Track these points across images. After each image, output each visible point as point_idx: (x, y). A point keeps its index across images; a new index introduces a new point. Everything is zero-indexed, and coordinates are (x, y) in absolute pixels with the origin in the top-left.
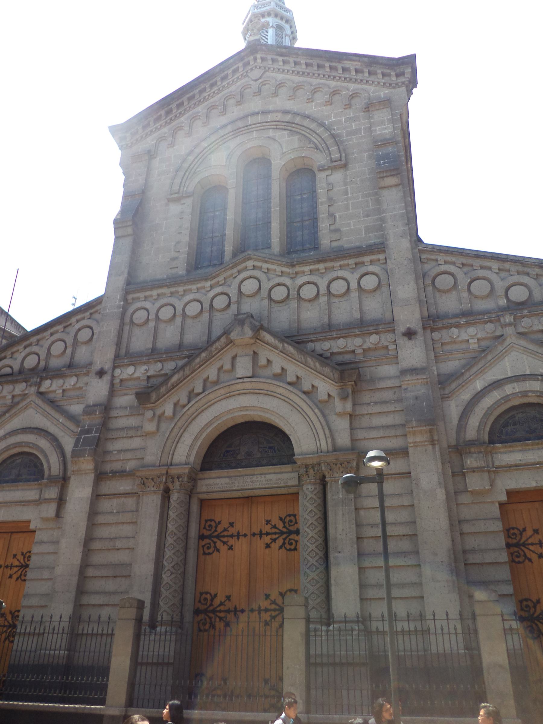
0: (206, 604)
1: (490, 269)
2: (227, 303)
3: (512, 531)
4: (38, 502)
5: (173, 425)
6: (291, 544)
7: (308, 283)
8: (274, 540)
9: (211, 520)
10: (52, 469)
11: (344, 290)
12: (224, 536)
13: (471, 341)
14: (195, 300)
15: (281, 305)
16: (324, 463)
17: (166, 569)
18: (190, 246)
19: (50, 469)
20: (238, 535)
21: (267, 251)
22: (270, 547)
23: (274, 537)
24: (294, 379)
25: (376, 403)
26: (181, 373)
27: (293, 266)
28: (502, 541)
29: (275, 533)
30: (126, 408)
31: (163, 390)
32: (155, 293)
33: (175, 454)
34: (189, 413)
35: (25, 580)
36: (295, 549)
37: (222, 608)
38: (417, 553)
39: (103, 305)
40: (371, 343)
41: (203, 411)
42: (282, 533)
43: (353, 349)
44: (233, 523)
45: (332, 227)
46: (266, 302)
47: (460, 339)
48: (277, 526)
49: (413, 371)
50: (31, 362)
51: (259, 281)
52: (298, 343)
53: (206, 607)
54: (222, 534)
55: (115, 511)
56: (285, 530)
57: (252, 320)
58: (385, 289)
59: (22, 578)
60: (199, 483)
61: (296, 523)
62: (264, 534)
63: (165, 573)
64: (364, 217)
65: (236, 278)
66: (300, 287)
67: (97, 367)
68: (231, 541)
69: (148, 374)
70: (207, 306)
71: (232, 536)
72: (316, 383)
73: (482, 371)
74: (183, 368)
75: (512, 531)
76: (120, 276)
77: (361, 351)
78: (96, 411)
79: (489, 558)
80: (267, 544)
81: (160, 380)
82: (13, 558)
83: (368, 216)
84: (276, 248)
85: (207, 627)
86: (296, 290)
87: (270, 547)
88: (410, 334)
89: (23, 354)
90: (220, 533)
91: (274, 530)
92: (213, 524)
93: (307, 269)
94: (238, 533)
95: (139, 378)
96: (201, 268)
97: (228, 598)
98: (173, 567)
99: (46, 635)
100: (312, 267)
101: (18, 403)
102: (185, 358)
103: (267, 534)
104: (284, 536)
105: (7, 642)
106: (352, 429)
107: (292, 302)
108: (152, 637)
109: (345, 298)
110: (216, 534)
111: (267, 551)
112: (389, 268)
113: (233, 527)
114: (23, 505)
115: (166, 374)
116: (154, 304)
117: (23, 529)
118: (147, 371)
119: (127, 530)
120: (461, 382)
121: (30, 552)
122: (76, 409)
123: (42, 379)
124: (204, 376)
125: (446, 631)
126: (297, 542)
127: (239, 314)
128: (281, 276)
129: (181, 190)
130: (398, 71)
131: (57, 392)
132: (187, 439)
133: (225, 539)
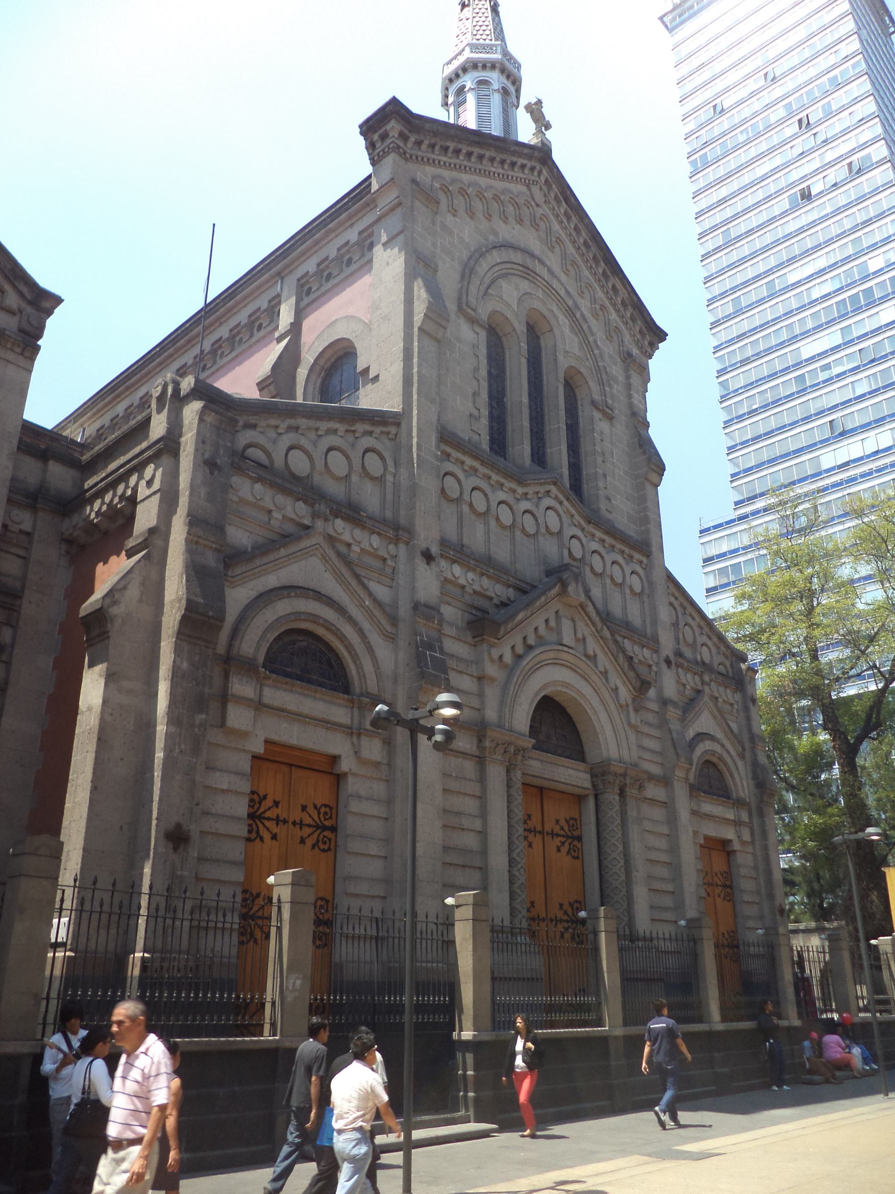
27: (589, 522)
50: (299, 463)
99: (391, 940)
114: (328, 728)
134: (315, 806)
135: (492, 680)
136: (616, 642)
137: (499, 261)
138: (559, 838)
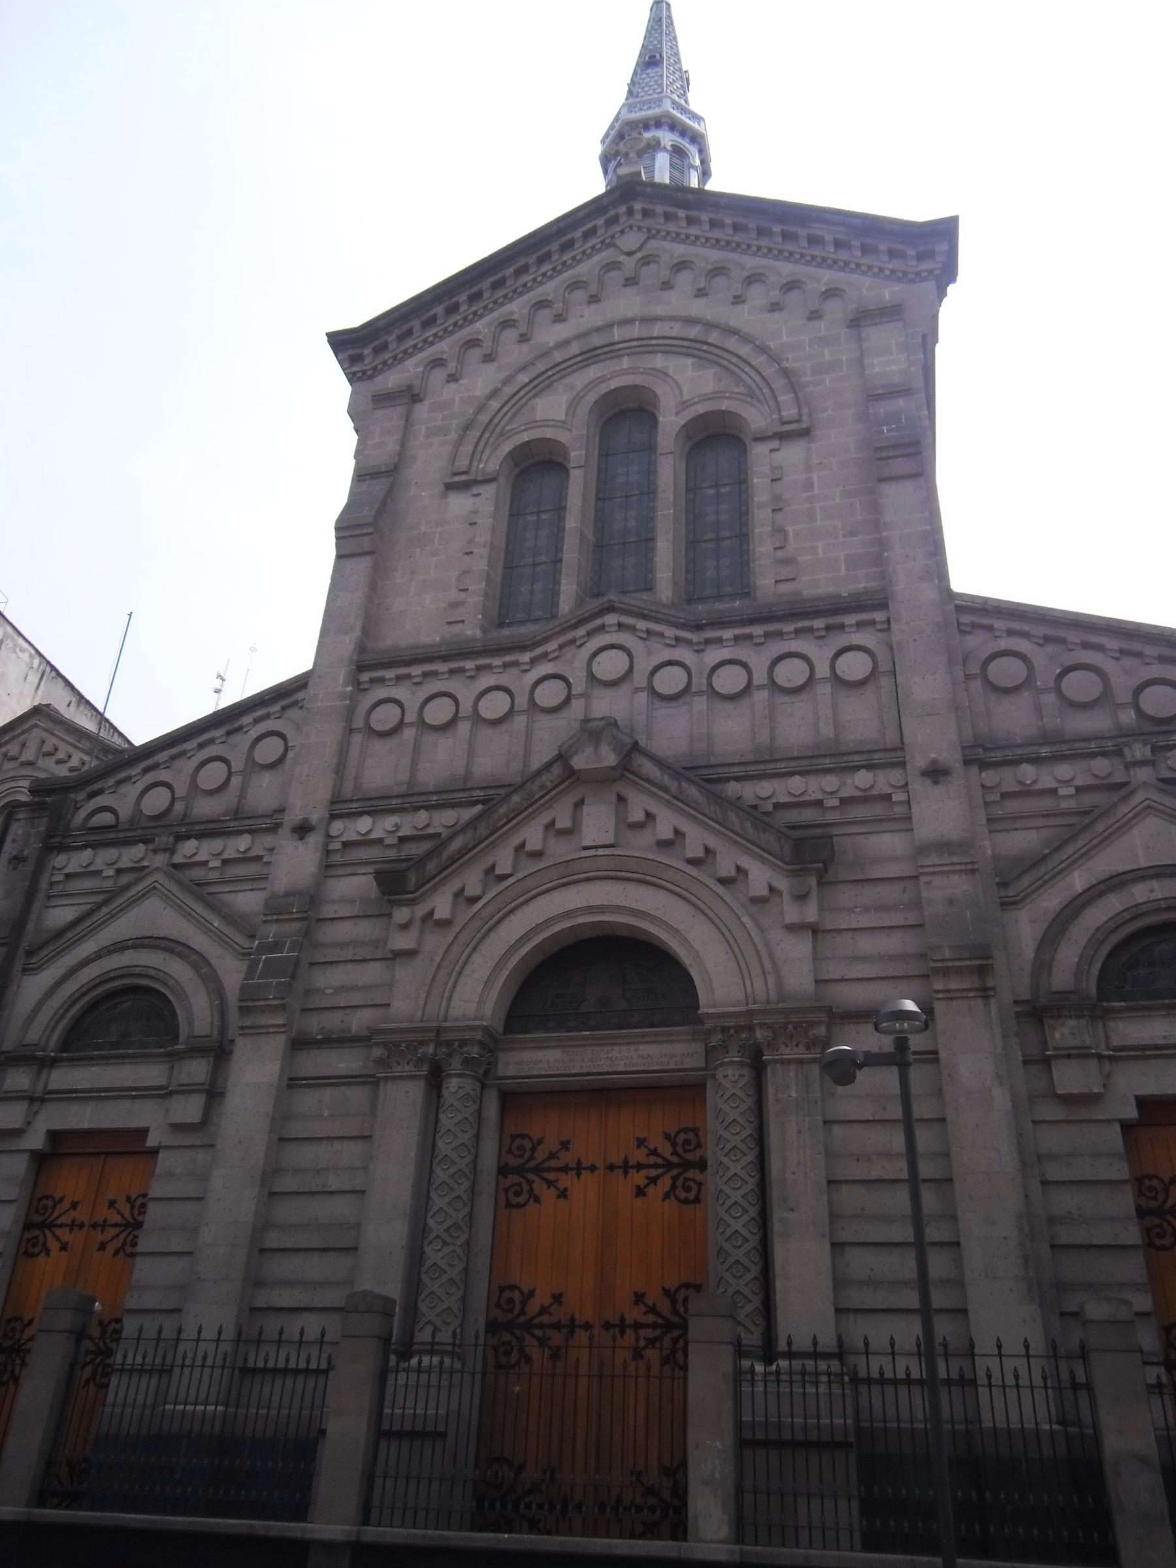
0: (511, 1311)
1: (1100, 648)
2: (563, 697)
3: (1147, 1183)
4: (164, 1093)
5: (450, 939)
6: (687, 1189)
7: (730, 662)
8: (654, 1180)
9: (523, 1136)
10: (196, 1023)
11: (800, 680)
12: (549, 1170)
13: (1061, 792)
14: (497, 688)
15: (674, 704)
16: (761, 1025)
17: (433, 1235)
18: (489, 580)
19: (190, 1024)
20: (579, 1169)
21: (645, 596)
22: (644, 1194)
23: (653, 1173)
24: (701, 853)
25: (866, 909)
26: (470, 833)
28: (1126, 1201)
29: (656, 1166)
30: (353, 901)
31: (431, 866)
32: (416, 671)
33: (455, 997)
34: (484, 914)
35: (133, 1255)
36: (697, 1200)
37: (545, 1319)
38: (954, 1218)
39: (311, 690)
40: (856, 787)
41: (512, 911)
42: (669, 1165)
43: (821, 797)
44: (568, 1142)
45: (780, 554)
46: (643, 697)
47: (1038, 786)
48: (660, 1151)
49: (942, 846)
50: (156, 802)
51: (630, 655)
52: (709, 781)
53: (510, 1316)
54: (546, 1165)
55: (326, 1114)
56: (675, 1159)
57: (615, 731)
58: (885, 681)
59: (128, 1251)
60: (502, 1057)
61: (699, 1146)
62: (633, 1167)
63: (430, 1243)
64: (844, 536)
65: (584, 648)
66: (714, 669)
67: (293, 817)
68: (565, 1181)
69: (400, 834)
70: (522, 702)
71: (565, 1169)
72: (745, 862)
73: (1086, 855)
74: (473, 822)
75: (1147, 1183)
76: (345, 634)
77: (836, 803)
78: (292, 905)
79: (1101, 1235)
80: (638, 1187)
81: (426, 846)
82: (109, 1208)
83: (852, 534)
84: (665, 590)
85: (514, 1357)
86: (706, 675)
87: (644, 1194)
88: (936, 773)
89: (140, 786)
90: (542, 1163)
91: (653, 1160)
92: (527, 1143)
93: (727, 634)
94: (579, 1163)
95: (380, 841)
96: (509, 625)
97: (558, 1298)
98: (447, 1230)
100: (738, 631)
101: (128, 886)
102: (475, 803)
103: (639, 1167)
104: (675, 1172)
105: (92, 1387)
106: (816, 958)
107: (696, 698)
108: (402, 1377)
109: (805, 696)
110: (532, 1164)
111: (639, 1202)
112: (895, 639)
113: (567, 1149)
115: (437, 835)
116: (414, 693)
117: (130, 1145)
118: (398, 827)
119: (351, 1152)
120: (1041, 874)
121: (144, 1196)
122: (248, 901)
123: (180, 838)
124: (516, 841)
125: (1025, 1381)
126: (700, 1185)
127: (586, 721)
128: (674, 646)
129: (474, 469)
130: (921, 249)
131: (211, 865)
132: (481, 965)
133: (551, 1176)
134: (128, 1199)
135: (411, 954)
136: (718, 799)
137: (527, 380)
138: (644, 1172)
